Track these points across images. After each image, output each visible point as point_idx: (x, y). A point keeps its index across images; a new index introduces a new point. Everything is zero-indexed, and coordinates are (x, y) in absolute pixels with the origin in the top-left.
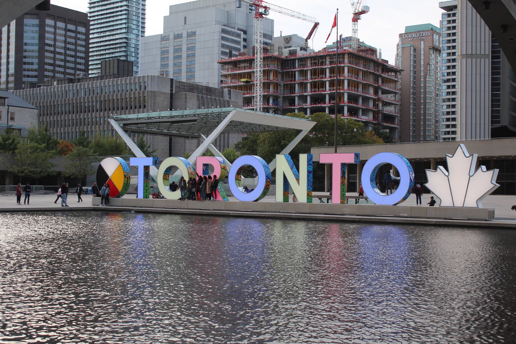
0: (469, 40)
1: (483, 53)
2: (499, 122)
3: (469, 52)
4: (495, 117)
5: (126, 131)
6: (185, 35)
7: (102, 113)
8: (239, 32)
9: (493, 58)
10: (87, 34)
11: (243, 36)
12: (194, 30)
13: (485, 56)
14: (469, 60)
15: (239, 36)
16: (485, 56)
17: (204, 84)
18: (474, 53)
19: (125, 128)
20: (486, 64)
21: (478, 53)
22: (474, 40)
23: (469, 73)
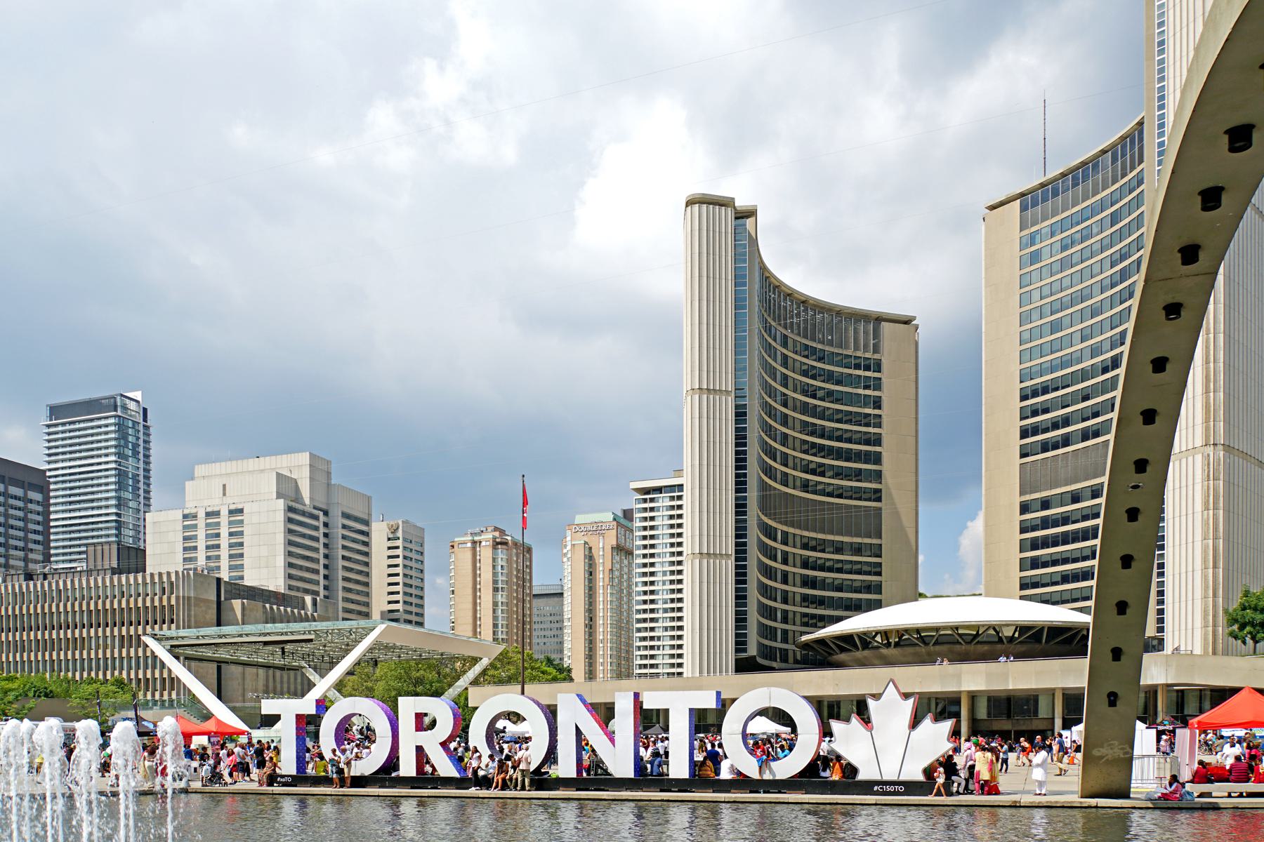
2: (745, 650)
4: (740, 644)
5: (177, 658)
6: (224, 512)
7: (92, 631)
8: (316, 512)
10: (46, 503)
11: (322, 518)
12: (240, 507)
15: (316, 518)
17: (271, 588)
19: (174, 651)
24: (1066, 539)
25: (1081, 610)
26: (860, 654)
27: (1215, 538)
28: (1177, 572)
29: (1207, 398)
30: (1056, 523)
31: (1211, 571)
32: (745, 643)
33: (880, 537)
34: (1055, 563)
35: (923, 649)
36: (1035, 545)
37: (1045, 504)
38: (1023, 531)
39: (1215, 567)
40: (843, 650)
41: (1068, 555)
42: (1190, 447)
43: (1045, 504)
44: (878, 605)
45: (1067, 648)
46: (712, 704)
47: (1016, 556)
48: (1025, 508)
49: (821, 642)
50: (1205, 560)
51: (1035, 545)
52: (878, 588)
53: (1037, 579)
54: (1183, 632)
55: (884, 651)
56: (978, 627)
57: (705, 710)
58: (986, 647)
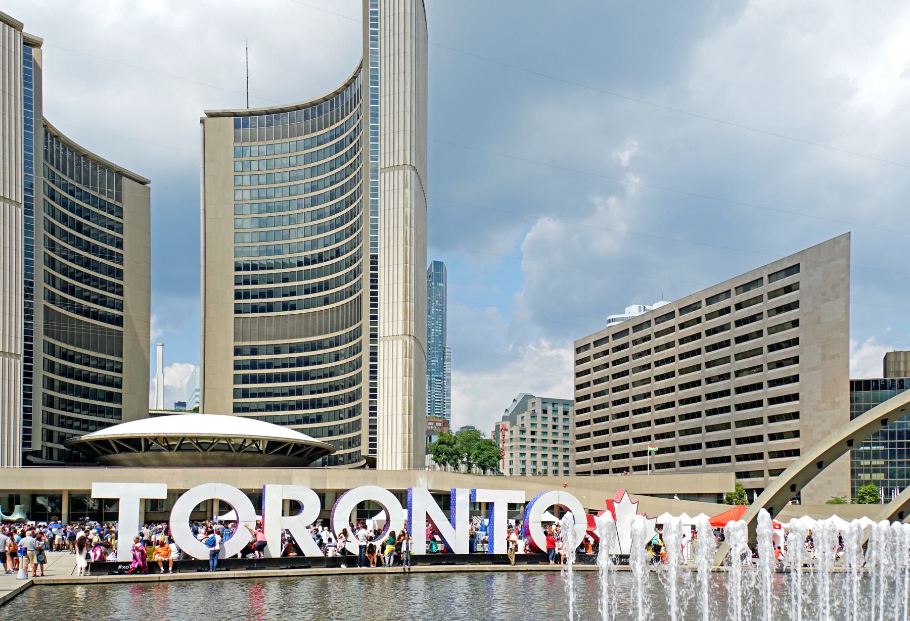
24: (269, 378)
27: (410, 395)
28: (386, 414)
30: (262, 366)
33: (121, 356)
34: (261, 395)
35: (200, 454)
36: (246, 379)
37: (254, 351)
38: (237, 367)
39: (409, 414)
41: (271, 391)
43: (254, 351)
45: (300, 459)
46: (164, 496)
47: (231, 386)
48: (237, 351)
49: (104, 442)
50: (404, 409)
51: (246, 379)
53: (247, 406)
54: (390, 455)
55: (164, 453)
57: (157, 500)
58: (249, 455)
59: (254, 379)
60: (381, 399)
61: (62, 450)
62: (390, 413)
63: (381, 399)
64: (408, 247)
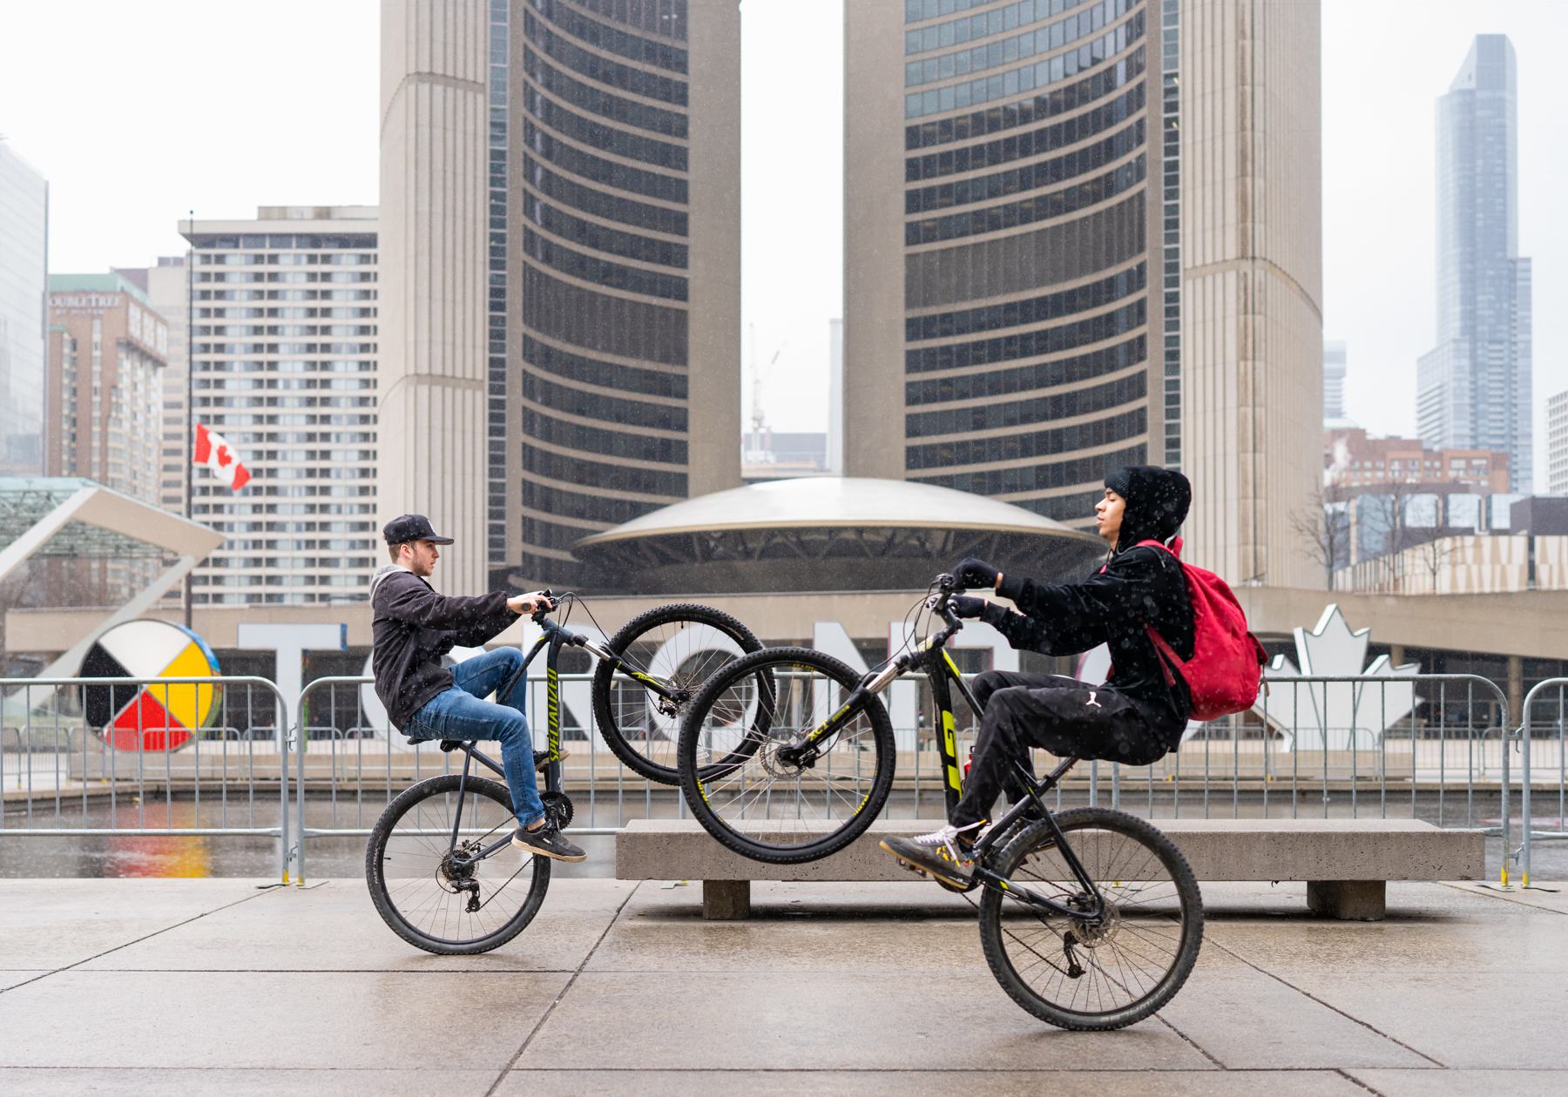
0: (438, 337)
1: (469, 375)
2: (501, 557)
3: (424, 370)
9: (492, 390)
13: (473, 383)
14: (437, 390)
16: (473, 383)
18: (449, 373)
20: (478, 403)
21: (459, 374)
22: (449, 339)
23: (437, 423)
25: (1022, 504)
26: (696, 568)
29: (1244, 185)
31: (1250, 456)
32: (501, 543)
40: (665, 560)
42: (1219, 258)
44: (678, 488)
49: (632, 544)
50: (1242, 440)
52: (678, 452)
55: (740, 564)
56: (895, 530)
59: (948, 390)
60: (1190, 418)
61: (568, 563)
62: (1210, 453)
63: (1190, 418)
64: (1248, 43)
